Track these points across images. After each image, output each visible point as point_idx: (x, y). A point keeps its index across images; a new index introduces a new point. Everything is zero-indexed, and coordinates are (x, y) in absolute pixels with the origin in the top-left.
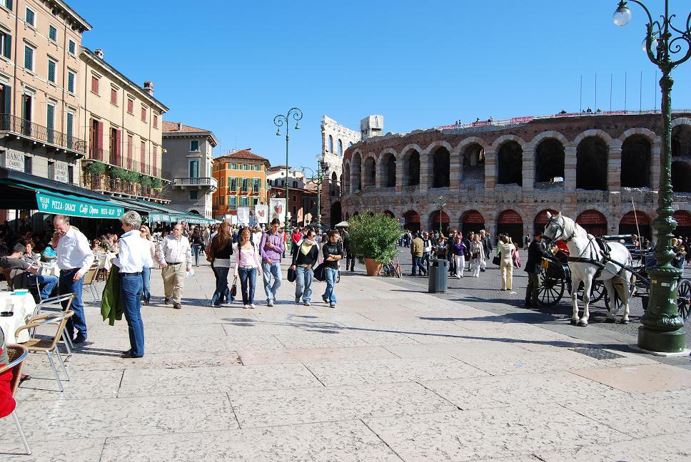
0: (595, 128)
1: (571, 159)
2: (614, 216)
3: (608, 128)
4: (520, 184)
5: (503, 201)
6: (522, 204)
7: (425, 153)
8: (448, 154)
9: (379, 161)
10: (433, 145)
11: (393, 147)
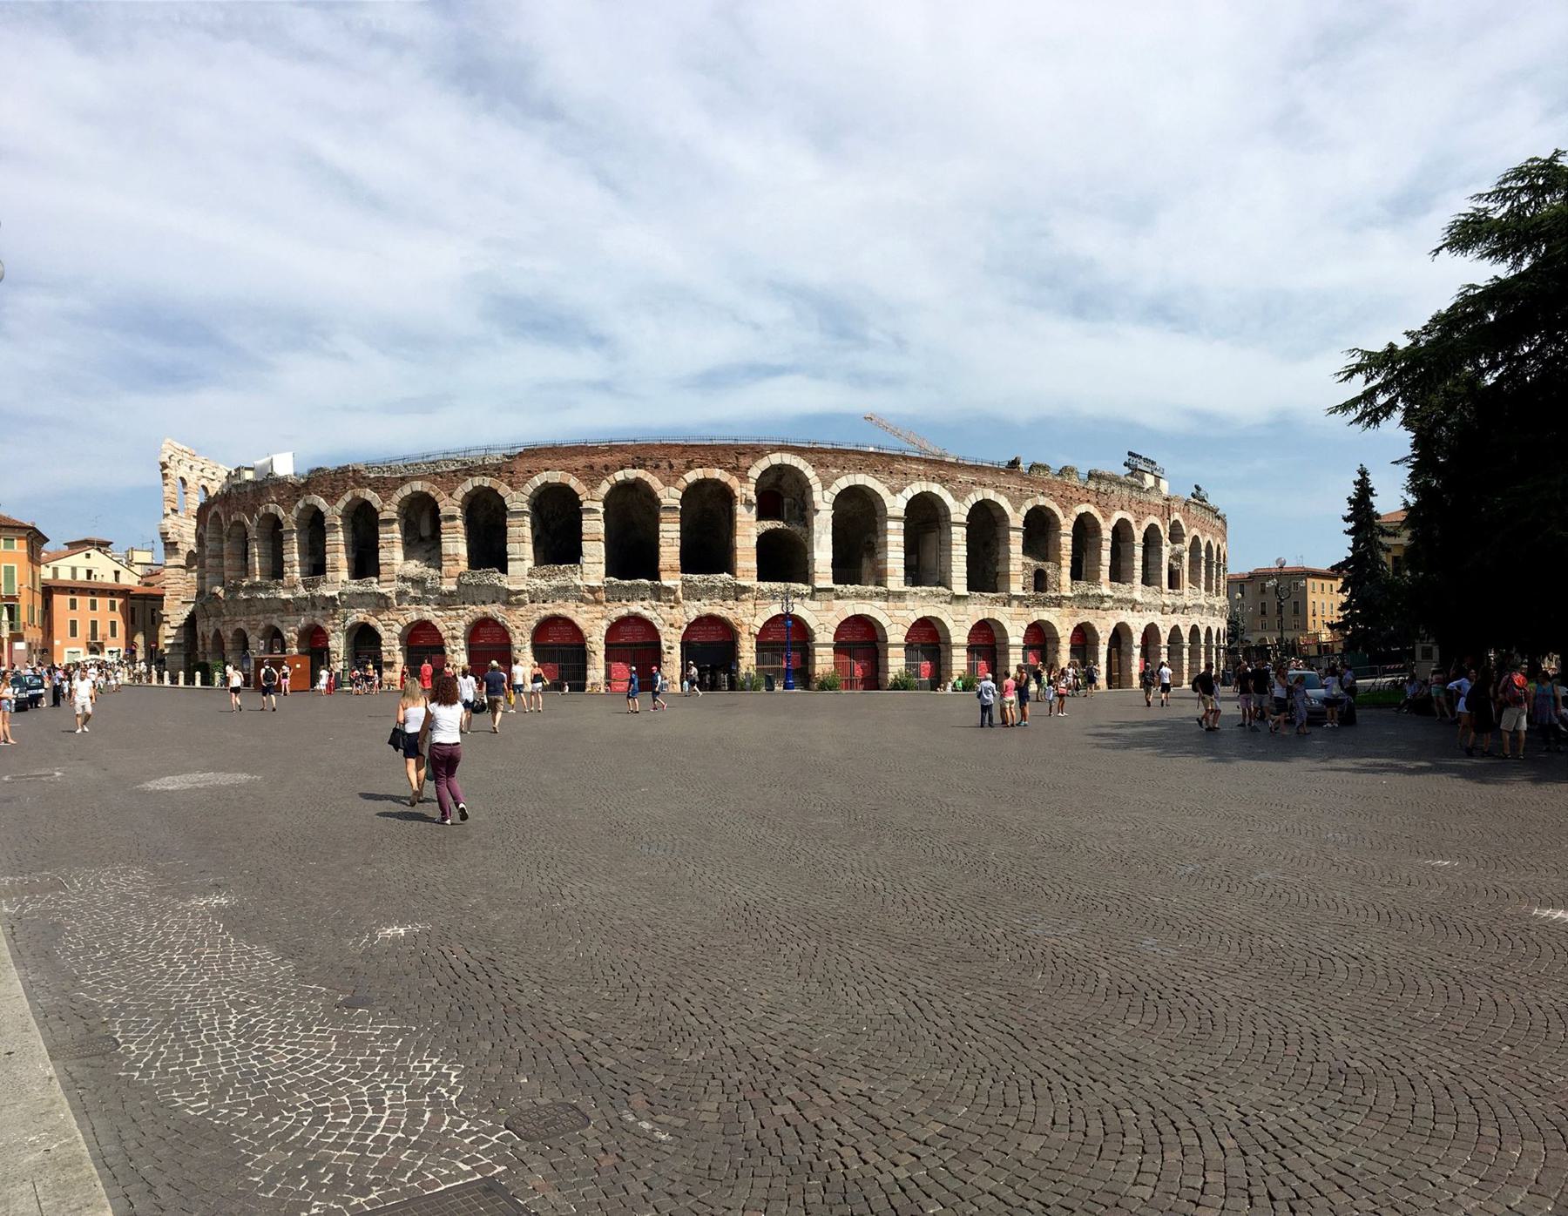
1: (594, 526)
3: (657, 467)
4: (504, 570)
7: (333, 512)
8: (375, 512)
10: (348, 497)
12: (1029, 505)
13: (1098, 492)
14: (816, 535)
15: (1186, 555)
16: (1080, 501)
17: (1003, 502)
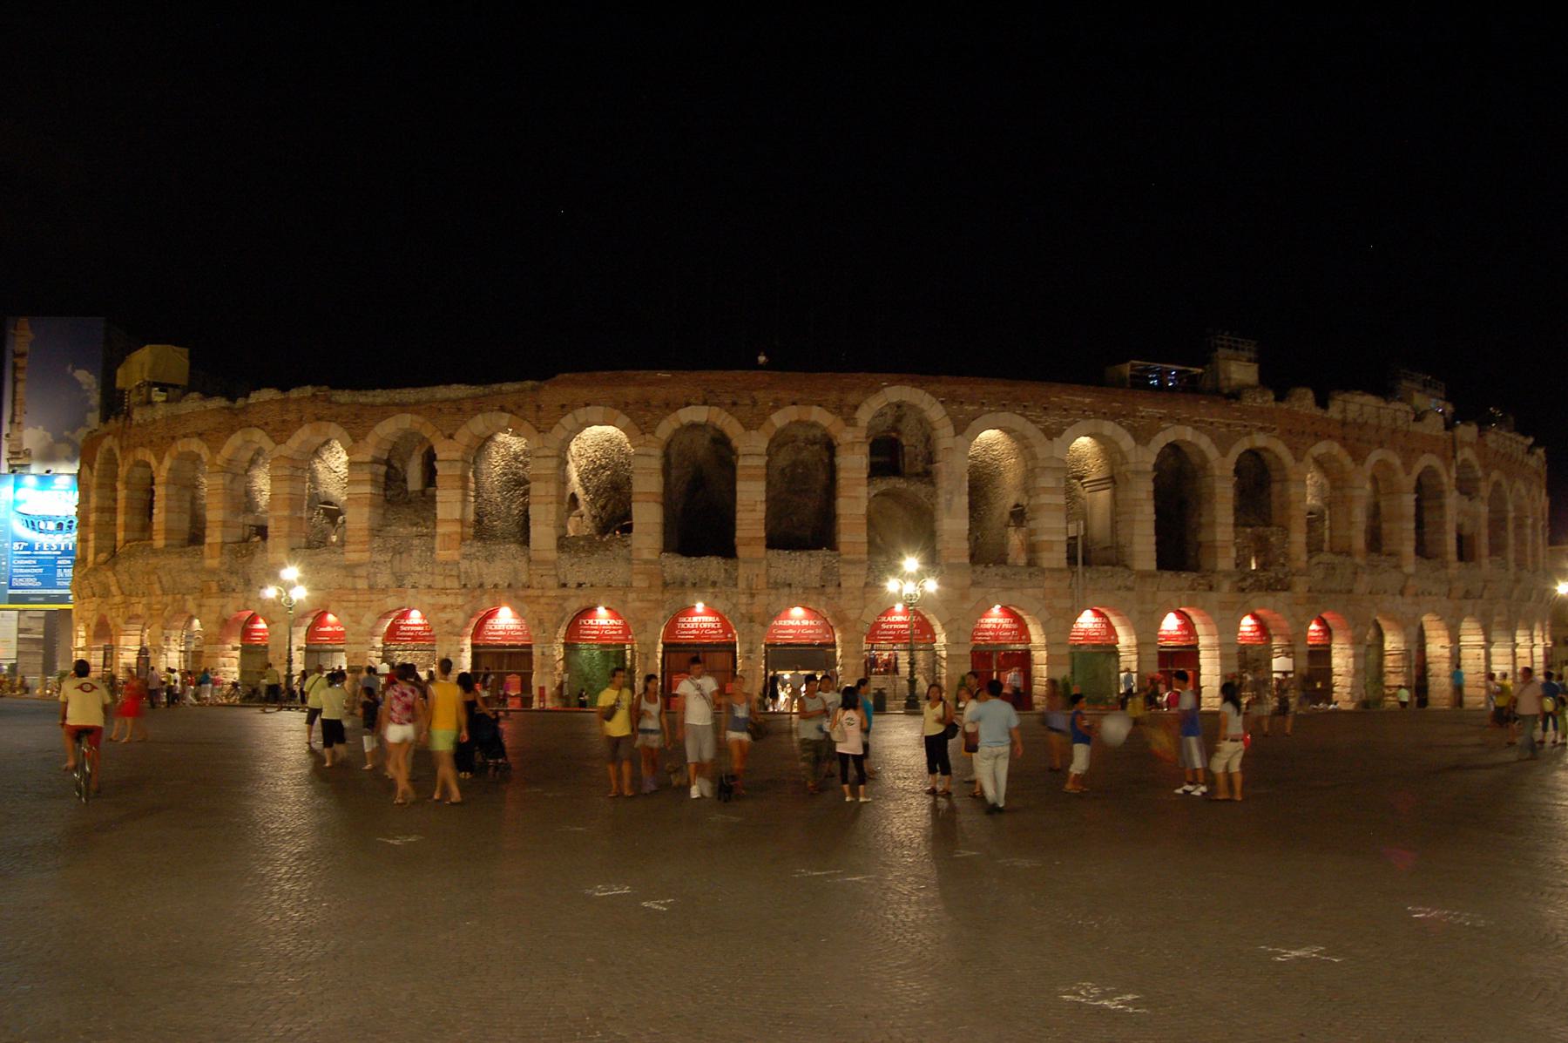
0: (705, 403)
2: (751, 620)
3: (734, 404)
5: (481, 585)
6: (530, 592)
9: (162, 474)
11: (200, 435)
12: (1243, 445)
13: (1344, 423)
14: (942, 500)
15: (1483, 510)
16: (1318, 437)
17: (1204, 443)
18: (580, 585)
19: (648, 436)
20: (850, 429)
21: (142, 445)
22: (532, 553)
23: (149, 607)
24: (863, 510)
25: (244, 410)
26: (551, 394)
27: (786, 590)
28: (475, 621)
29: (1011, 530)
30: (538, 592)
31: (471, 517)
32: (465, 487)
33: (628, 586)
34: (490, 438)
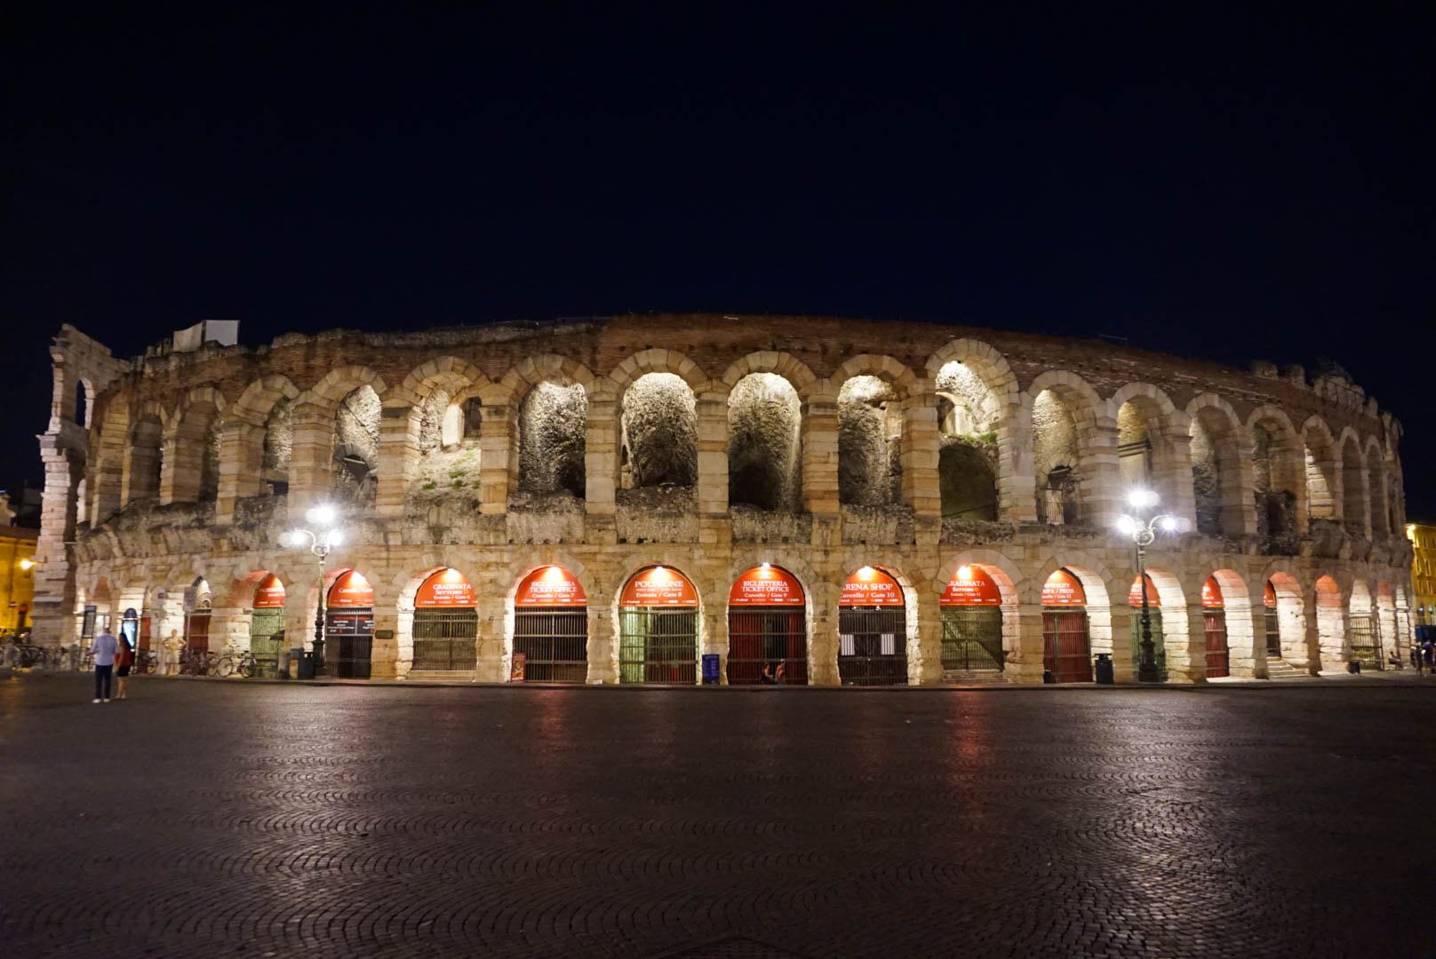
0: (774, 348)
2: (825, 579)
3: (804, 350)
4: (580, 493)
5: (530, 541)
6: (585, 548)
13: (1324, 400)
18: (640, 541)
19: (715, 382)
20: (921, 381)
21: (152, 399)
22: (587, 506)
23: (153, 568)
24: (936, 465)
25: (266, 358)
26: (610, 339)
27: (862, 547)
28: (520, 580)
29: (1049, 493)
30: (595, 549)
31: (517, 469)
32: (511, 436)
33: (695, 541)
34: (535, 386)
